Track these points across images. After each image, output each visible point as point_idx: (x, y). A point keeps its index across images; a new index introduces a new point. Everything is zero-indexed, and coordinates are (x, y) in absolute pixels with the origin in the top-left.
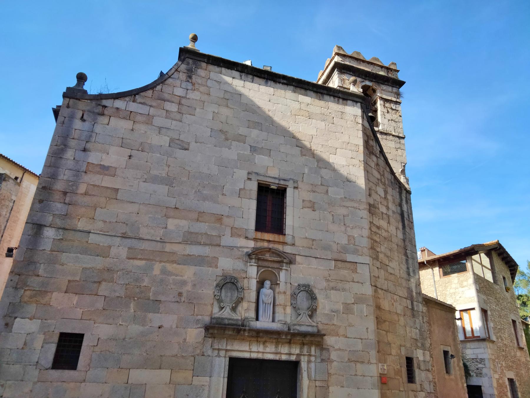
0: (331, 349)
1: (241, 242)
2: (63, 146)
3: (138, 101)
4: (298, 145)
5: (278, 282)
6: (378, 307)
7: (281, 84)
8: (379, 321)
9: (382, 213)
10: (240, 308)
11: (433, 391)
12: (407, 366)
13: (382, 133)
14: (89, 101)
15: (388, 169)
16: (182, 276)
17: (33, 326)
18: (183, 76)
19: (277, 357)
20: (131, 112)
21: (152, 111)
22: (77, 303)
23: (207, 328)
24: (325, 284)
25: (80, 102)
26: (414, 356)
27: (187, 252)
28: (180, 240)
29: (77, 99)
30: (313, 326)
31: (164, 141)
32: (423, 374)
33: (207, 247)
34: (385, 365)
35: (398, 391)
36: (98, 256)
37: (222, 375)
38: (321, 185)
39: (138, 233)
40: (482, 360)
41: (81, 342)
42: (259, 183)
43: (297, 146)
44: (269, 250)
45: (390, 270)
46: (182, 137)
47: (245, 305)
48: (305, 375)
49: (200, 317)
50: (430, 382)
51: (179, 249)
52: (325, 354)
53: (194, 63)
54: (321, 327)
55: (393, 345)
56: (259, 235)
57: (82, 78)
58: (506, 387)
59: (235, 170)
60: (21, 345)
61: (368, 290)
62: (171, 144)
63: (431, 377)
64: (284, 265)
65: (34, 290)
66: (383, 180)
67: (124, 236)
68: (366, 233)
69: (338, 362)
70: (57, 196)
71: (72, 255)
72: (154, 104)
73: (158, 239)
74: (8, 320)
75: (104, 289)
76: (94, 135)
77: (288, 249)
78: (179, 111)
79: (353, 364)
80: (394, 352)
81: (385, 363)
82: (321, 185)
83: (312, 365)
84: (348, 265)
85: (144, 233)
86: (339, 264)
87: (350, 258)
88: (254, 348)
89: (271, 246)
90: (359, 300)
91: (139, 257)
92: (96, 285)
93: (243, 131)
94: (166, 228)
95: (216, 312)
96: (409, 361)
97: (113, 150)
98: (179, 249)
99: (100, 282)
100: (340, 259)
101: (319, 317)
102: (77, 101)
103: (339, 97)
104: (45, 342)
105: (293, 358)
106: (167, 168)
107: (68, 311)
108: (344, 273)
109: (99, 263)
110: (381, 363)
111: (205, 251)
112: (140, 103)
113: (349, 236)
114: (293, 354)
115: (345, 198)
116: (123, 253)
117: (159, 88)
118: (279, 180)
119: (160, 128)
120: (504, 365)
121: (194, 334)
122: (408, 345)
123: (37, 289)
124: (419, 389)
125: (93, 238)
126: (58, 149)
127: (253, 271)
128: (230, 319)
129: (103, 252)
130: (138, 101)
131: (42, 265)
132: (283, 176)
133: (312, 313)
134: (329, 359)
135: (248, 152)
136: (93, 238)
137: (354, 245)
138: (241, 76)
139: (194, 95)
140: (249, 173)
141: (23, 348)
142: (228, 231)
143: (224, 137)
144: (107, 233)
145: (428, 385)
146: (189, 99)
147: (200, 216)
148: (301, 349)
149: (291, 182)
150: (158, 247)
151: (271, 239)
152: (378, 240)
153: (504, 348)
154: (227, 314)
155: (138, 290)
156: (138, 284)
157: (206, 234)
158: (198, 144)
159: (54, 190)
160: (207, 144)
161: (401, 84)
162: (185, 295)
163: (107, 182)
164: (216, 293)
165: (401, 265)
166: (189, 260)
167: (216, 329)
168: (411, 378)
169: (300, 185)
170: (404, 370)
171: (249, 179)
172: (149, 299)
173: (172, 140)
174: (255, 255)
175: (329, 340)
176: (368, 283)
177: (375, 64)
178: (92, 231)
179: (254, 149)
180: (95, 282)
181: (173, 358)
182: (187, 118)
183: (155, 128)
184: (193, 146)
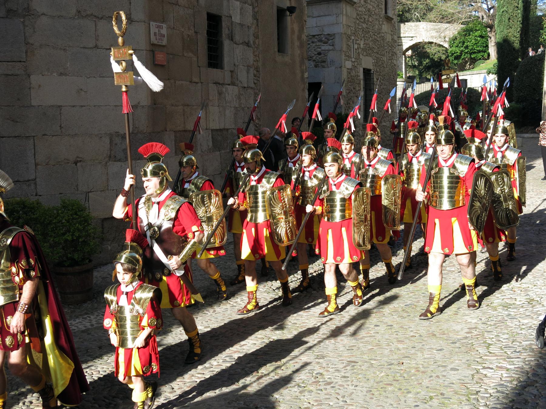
11: (252, 85)
12: (208, 33)
26: (224, 13)
32: (239, 50)
34: (164, 26)
35: (188, 83)
40: (330, 37)
50: (248, 66)
58: (359, 84)
81: (163, 22)
96: (214, 22)
110: (155, 21)
120: (362, 46)
124: (228, 80)
153: (366, 17)
168: (215, 59)
170: (202, 38)
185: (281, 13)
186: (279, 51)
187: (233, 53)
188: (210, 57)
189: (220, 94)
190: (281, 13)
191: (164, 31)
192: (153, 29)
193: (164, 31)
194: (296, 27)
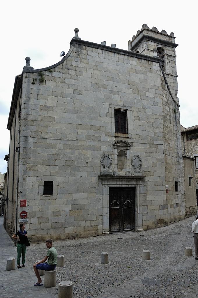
0: (148, 181)
1: (109, 138)
2: (28, 98)
3: (57, 71)
4: (131, 88)
5: (126, 155)
6: (166, 163)
7: (121, 55)
8: (166, 168)
9: (168, 119)
10: (111, 167)
13: (167, 74)
14: (35, 73)
15: (171, 96)
16: (87, 155)
17: (34, 179)
18: (75, 54)
19: (127, 186)
21: (64, 76)
22: (48, 169)
23: (99, 177)
24: (145, 155)
25: (31, 74)
27: (88, 145)
28: (84, 139)
29: (30, 73)
30: (141, 173)
31: (70, 91)
33: (95, 142)
36: (52, 149)
37: (107, 194)
38: (142, 108)
41: (52, 184)
43: (131, 89)
44: (122, 141)
45: (171, 146)
46: (79, 88)
47: (113, 166)
48: (138, 192)
49: (96, 172)
51: (84, 143)
52: (145, 184)
53: (79, 47)
54: (144, 172)
55: (171, 177)
56: (117, 135)
57: (28, 60)
59: (104, 103)
61: (163, 156)
62: (74, 93)
63: (184, 188)
64: (128, 147)
66: (168, 103)
67: (61, 139)
68: (162, 130)
69: (150, 186)
71: (42, 149)
72: (64, 72)
73: (75, 140)
74: (24, 177)
75: (57, 163)
76: (40, 91)
77: (129, 140)
78: (76, 74)
79: (156, 186)
80: (171, 180)
82: (142, 108)
83: (141, 188)
84: (154, 146)
85: (69, 137)
86: (151, 145)
87: (155, 142)
88: (118, 183)
89: (122, 139)
90: (159, 160)
93: (105, 83)
94: (77, 134)
95: (103, 170)
96: (176, 183)
97: (50, 97)
98: (84, 143)
100: (151, 143)
101: (143, 169)
102: (30, 74)
103: (149, 60)
104: (39, 185)
105: (133, 186)
106: (74, 105)
107: (46, 173)
108: (153, 149)
109: (53, 152)
112: (58, 72)
114: (133, 184)
115: (153, 114)
116: (62, 147)
117: (65, 62)
118: (124, 107)
119: (68, 84)
121: (95, 179)
122: (176, 177)
126: (26, 100)
127: (116, 151)
128: (108, 172)
129: (53, 147)
130: (57, 71)
131: (31, 154)
132: (125, 105)
133: (140, 167)
134: (147, 185)
135: (109, 94)
136: (48, 141)
137: (157, 136)
138: (102, 52)
139: (82, 65)
140: (110, 105)
141: (32, 188)
142: (103, 134)
143: (97, 86)
145: (182, 192)
146: (79, 67)
147: (91, 127)
148: (136, 182)
149: (129, 107)
150: (76, 143)
151: (122, 136)
152: (166, 133)
154: (106, 169)
155: (70, 162)
157: (94, 135)
159: (29, 120)
160: (90, 91)
161: (176, 45)
162: (89, 163)
163: (50, 114)
164: (101, 162)
165: (175, 143)
166: (89, 148)
167: (103, 178)
168: (177, 190)
169: (133, 109)
172: (75, 166)
173: (74, 90)
174: (116, 144)
175: (147, 178)
176: (162, 153)
177: (164, 34)
178: (48, 138)
179: (111, 92)
182: (80, 78)
183: (66, 84)
184: (84, 93)
185: (190, 178)
186: (189, 186)
187: (180, 188)
188: (176, 189)
189: (178, 196)
190: (190, 178)
191: (168, 187)
192: (166, 187)
193: (168, 187)
194: (193, 180)
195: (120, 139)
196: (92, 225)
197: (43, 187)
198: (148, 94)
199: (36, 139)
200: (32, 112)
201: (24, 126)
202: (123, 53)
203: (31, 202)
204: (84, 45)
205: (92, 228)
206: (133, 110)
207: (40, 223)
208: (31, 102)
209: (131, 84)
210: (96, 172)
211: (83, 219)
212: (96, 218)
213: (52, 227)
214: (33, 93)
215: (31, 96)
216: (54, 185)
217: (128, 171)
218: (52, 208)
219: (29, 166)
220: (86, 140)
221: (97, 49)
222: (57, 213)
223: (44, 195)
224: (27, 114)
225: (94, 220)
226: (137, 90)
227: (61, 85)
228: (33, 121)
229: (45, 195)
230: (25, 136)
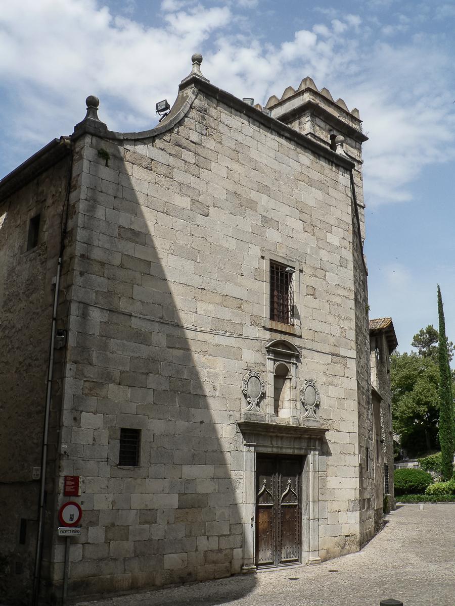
4: (302, 219)
16: (214, 368)
20: (152, 160)
21: (172, 161)
25: (103, 142)
27: (216, 342)
39: (173, 318)
42: (271, 263)
43: (300, 220)
46: (201, 198)
49: (231, 413)
54: (322, 421)
57: (92, 104)
59: (250, 245)
60: (91, 442)
65: (93, 382)
70: (96, 268)
77: (295, 342)
82: (321, 269)
84: (341, 359)
91: (177, 346)
92: (144, 376)
93: (253, 195)
99: (147, 374)
104: (110, 438)
108: (338, 367)
109: (144, 351)
111: (231, 342)
113: (342, 328)
115: (339, 285)
123: (95, 380)
125: (135, 323)
127: (270, 366)
135: (259, 223)
136: (135, 323)
139: (210, 144)
141: (93, 444)
142: (248, 321)
144: (146, 317)
146: (204, 147)
149: (297, 264)
155: (180, 384)
156: (179, 377)
158: (217, 209)
162: (218, 388)
171: (263, 257)
175: (328, 436)
178: (133, 314)
180: (143, 373)
181: (214, 454)
182: (204, 173)
184: (212, 211)
195: (279, 337)
196: (222, 547)
197: (119, 445)
198: (331, 238)
199: (106, 314)
200: (101, 241)
201: (82, 274)
202: (288, 135)
203: (90, 482)
204: (216, 98)
205: (220, 556)
206: (305, 272)
207: (108, 541)
208: (100, 213)
209: (301, 208)
210: (231, 413)
211: (203, 531)
212: (230, 530)
213: (135, 551)
214: (104, 190)
215: (101, 198)
216: (144, 438)
217: (287, 415)
218: (137, 501)
219: (87, 384)
220: (213, 332)
221: (240, 112)
222: (148, 516)
223: (120, 464)
224: (89, 243)
225: (225, 536)
226: (311, 227)
227: (165, 181)
228: (102, 264)
229: (122, 467)
230: (83, 300)
